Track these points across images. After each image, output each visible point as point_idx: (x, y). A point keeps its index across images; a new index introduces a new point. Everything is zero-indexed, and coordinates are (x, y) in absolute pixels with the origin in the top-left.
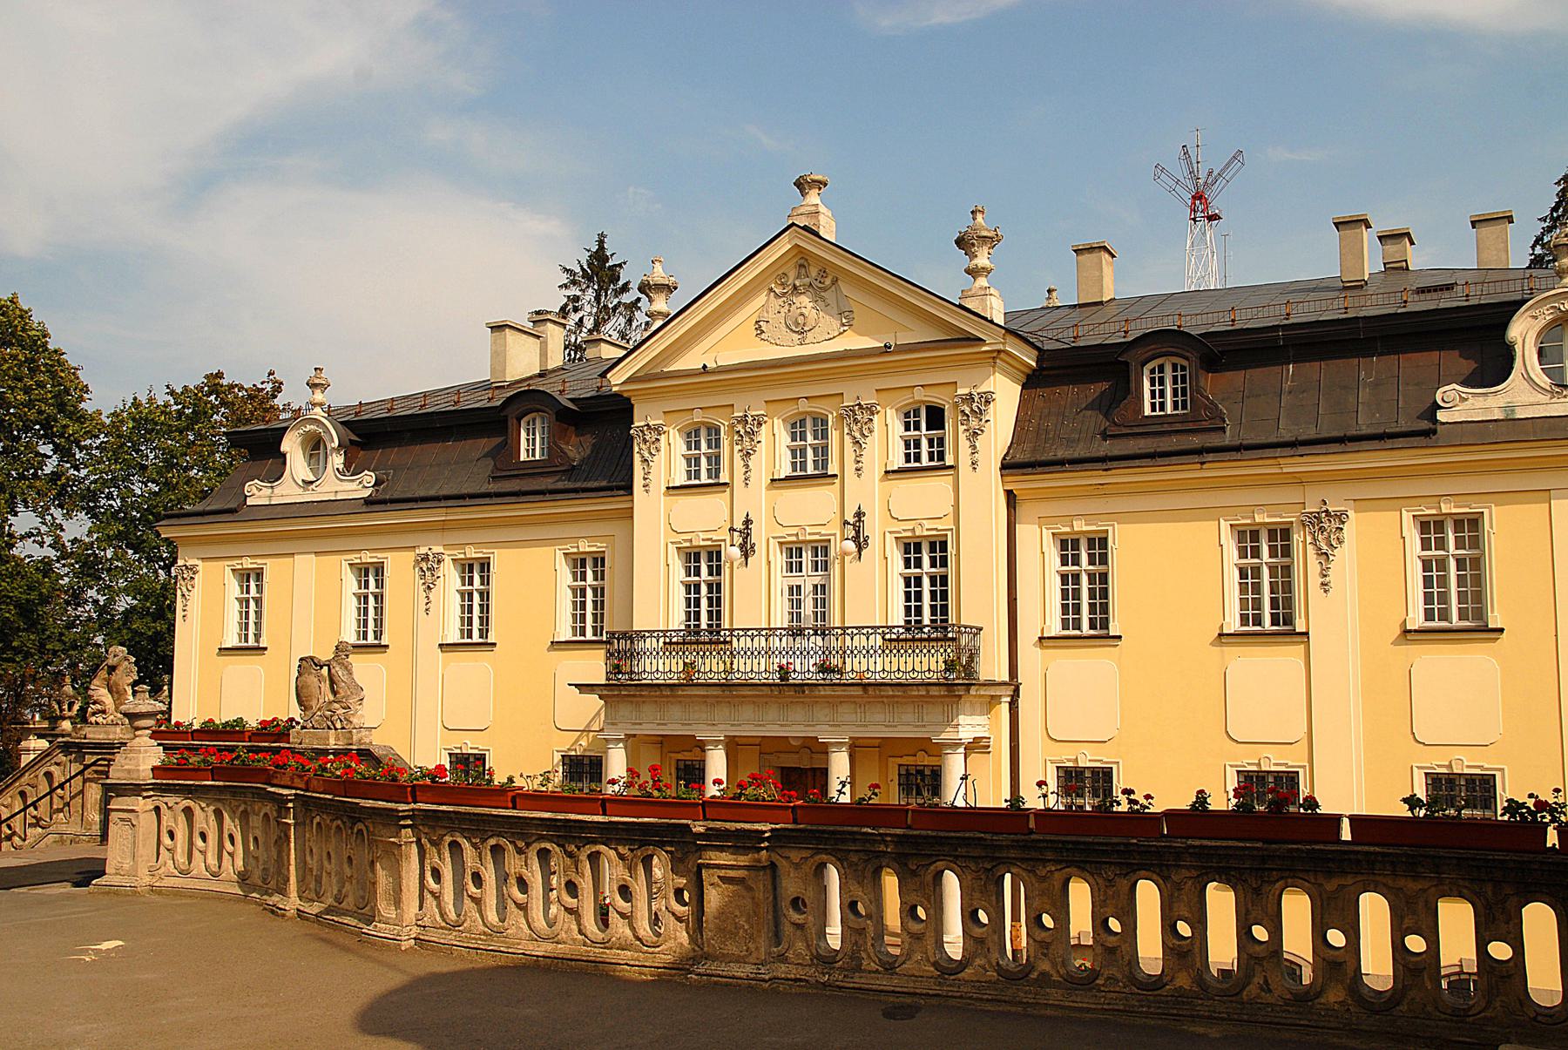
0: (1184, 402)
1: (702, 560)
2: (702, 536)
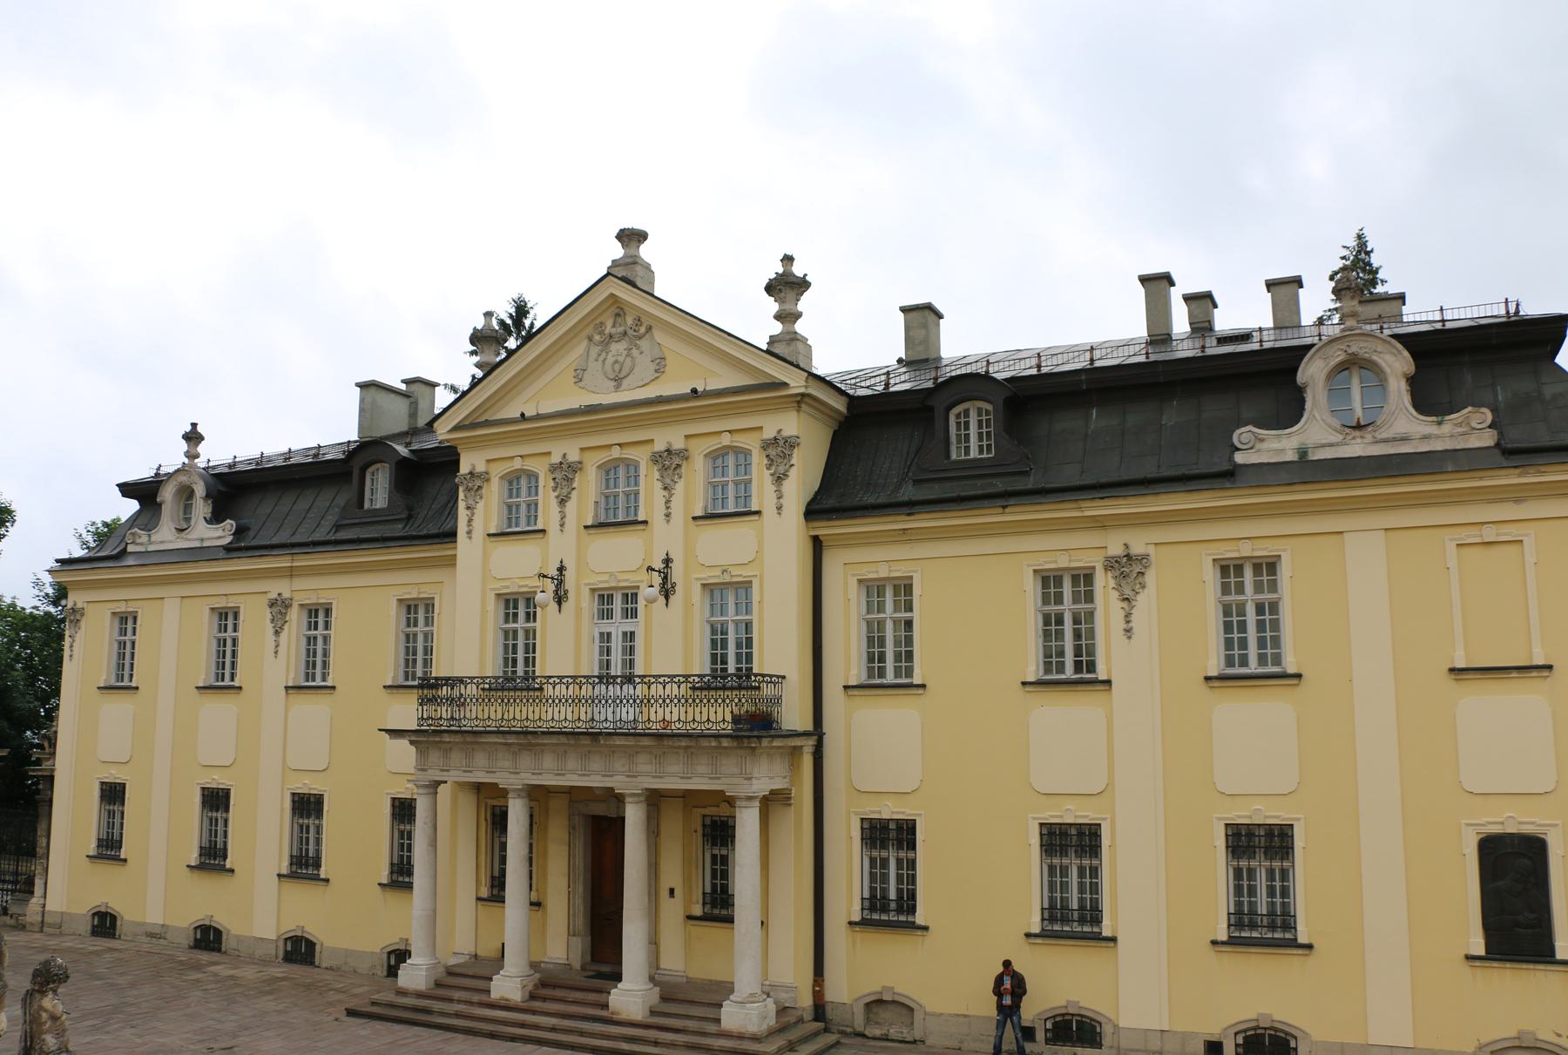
0: (989, 446)
1: (516, 606)
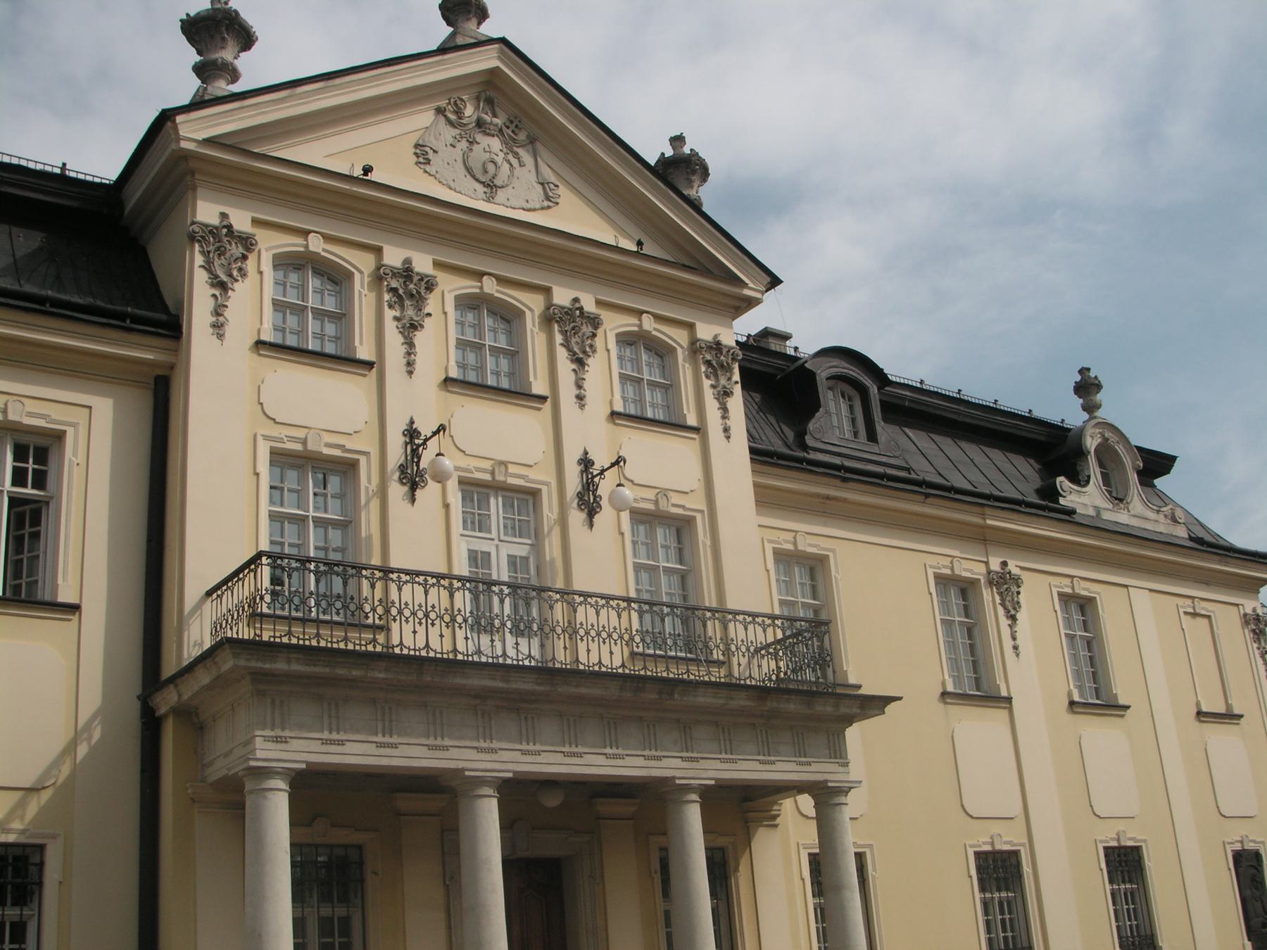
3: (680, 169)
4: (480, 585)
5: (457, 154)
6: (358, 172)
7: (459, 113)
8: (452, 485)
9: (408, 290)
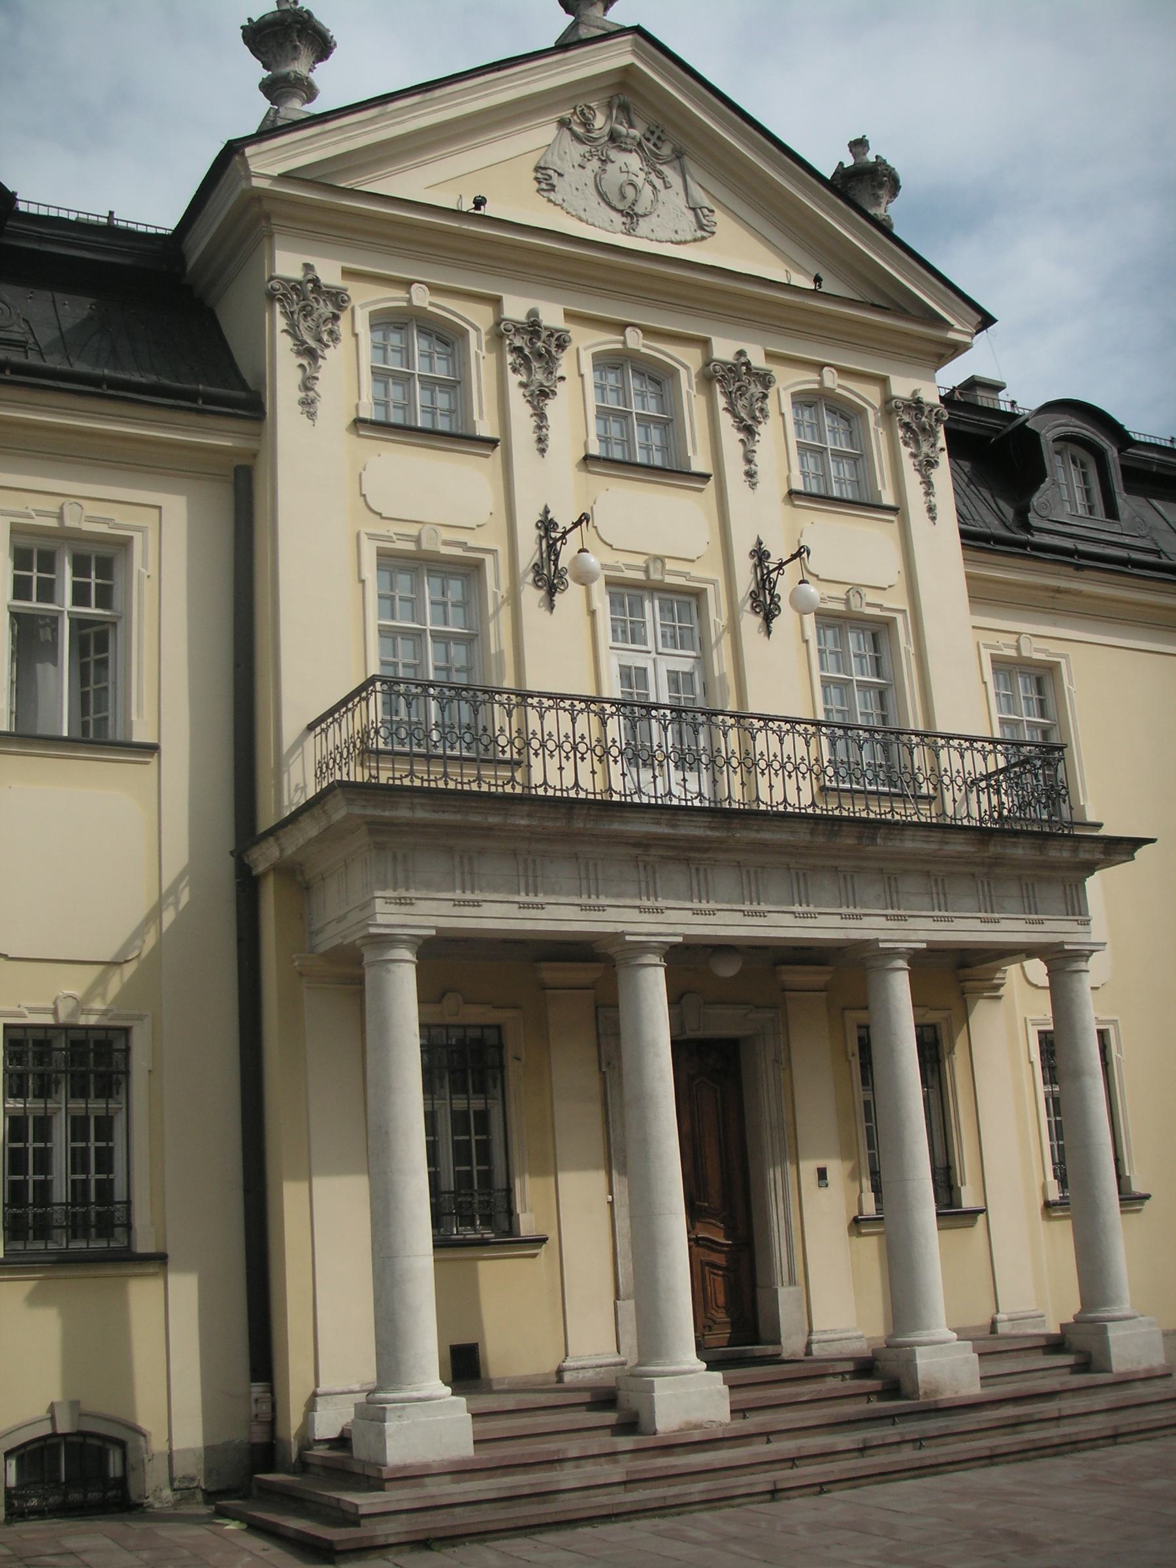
2: (446, 534)
3: (864, 182)
4: (636, 709)
5: (588, 175)
6: (468, 206)
7: (587, 124)
8: (599, 588)
9: (535, 349)
